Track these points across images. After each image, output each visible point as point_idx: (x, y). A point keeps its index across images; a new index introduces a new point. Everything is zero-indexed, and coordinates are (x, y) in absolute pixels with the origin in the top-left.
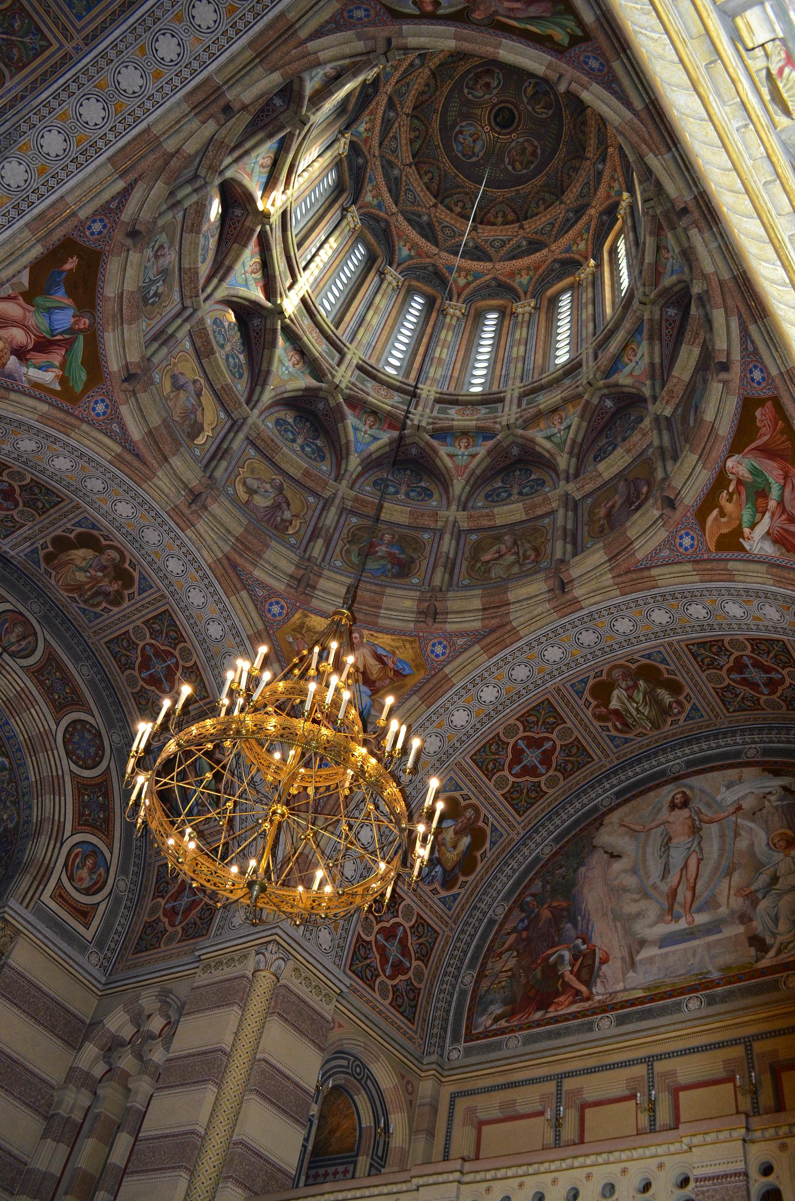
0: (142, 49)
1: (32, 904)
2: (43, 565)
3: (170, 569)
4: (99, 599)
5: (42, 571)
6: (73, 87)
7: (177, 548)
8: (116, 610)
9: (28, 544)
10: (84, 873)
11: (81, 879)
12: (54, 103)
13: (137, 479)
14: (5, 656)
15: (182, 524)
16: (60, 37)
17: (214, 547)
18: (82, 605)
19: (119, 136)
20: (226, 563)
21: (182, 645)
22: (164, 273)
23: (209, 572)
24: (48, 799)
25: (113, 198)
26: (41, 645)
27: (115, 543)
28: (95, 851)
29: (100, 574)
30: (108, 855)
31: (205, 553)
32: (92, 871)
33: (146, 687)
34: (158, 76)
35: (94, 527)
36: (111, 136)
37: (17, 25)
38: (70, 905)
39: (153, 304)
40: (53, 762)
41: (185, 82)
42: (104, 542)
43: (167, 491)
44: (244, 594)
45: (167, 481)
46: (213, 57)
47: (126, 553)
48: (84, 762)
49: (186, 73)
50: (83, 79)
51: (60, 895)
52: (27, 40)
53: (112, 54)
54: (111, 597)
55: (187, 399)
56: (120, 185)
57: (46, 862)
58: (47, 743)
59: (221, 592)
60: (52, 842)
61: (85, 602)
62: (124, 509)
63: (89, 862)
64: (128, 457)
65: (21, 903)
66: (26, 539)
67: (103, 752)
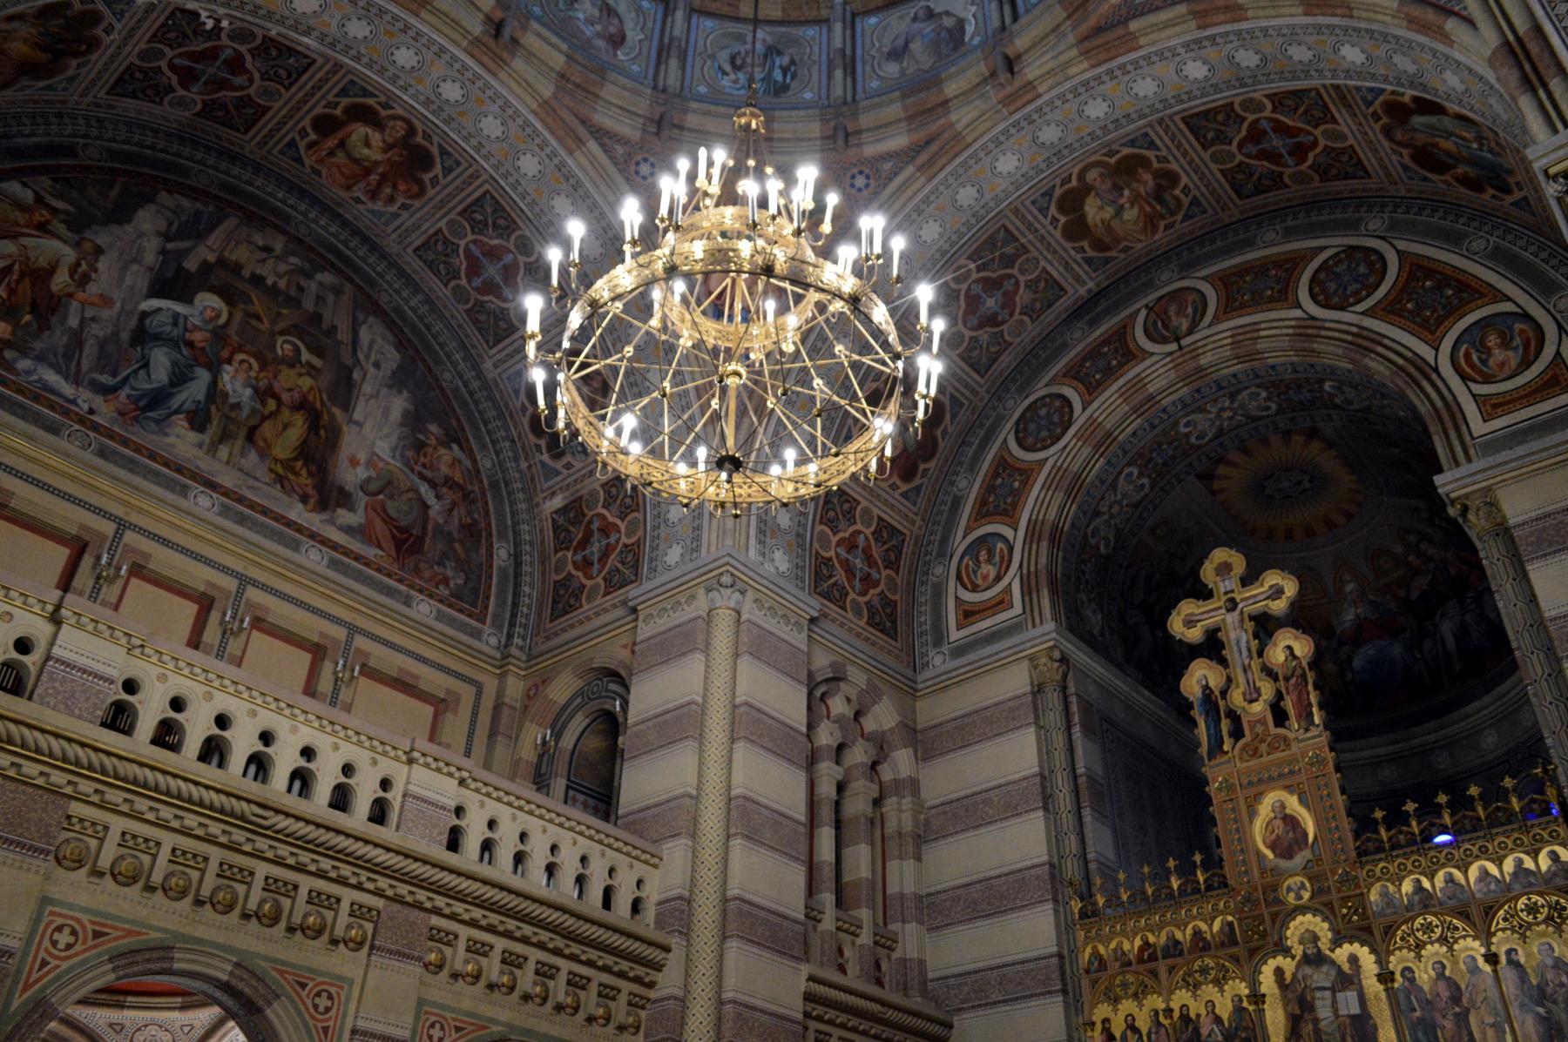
0: (460, 114)
1: (1472, 452)
2: (1113, 253)
3: (1102, 115)
4: (1167, 197)
5: (1123, 256)
6: (511, 180)
7: (1068, 105)
8: (1184, 180)
9: (1075, 267)
10: (1498, 355)
11: (1502, 365)
12: (529, 199)
13: (957, 149)
14: (1184, 342)
15: (1030, 96)
16: (479, 181)
17: (1063, 58)
18: (1179, 217)
19: (545, 143)
20: (1087, 45)
21: (1237, 108)
22: (772, 51)
23: (1104, 68)
24: (1373, 364)
25: (607, 150)
26: (1206, 288)
27: (1076, 171)
28: (1484, 324)
29: (1126, 193)
30: (1507, 307)
31: (1073, 70)
32: (1506, 344)
33: (1309, 162)
34: (480, 102)
35: (1048, 194)
36: (548, 150)
37: (479, 217)
38: (1519, 398)
39: (793, 77)
40: (1336, 335)
41: (478, 77)
42: (1074, 183)
43: (975, 114)
44: (1134, 25)
45: (965, 110)
46: (443, 50)
47: (1093, 159)
48: (1365, 287)
49: (469, 75)
50: (503, 170)
51: (1491, 407)
52: (489, 210)
53: (474, 142)
54: (1163, 182)
55: (923, 37)
56: (592, 145)
57: (1439, 404)
58: (1310, 331)
59: (1133, 56)
60: (1425, 384)
61: (1173, 213)
62: (1008, 163)
63: (1492, 340)
64: (923, 157)
65: (1457, 464)
66: (1067, 266)
67: (1375, 251)
